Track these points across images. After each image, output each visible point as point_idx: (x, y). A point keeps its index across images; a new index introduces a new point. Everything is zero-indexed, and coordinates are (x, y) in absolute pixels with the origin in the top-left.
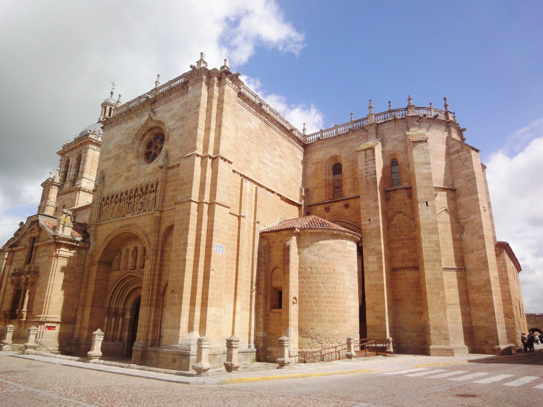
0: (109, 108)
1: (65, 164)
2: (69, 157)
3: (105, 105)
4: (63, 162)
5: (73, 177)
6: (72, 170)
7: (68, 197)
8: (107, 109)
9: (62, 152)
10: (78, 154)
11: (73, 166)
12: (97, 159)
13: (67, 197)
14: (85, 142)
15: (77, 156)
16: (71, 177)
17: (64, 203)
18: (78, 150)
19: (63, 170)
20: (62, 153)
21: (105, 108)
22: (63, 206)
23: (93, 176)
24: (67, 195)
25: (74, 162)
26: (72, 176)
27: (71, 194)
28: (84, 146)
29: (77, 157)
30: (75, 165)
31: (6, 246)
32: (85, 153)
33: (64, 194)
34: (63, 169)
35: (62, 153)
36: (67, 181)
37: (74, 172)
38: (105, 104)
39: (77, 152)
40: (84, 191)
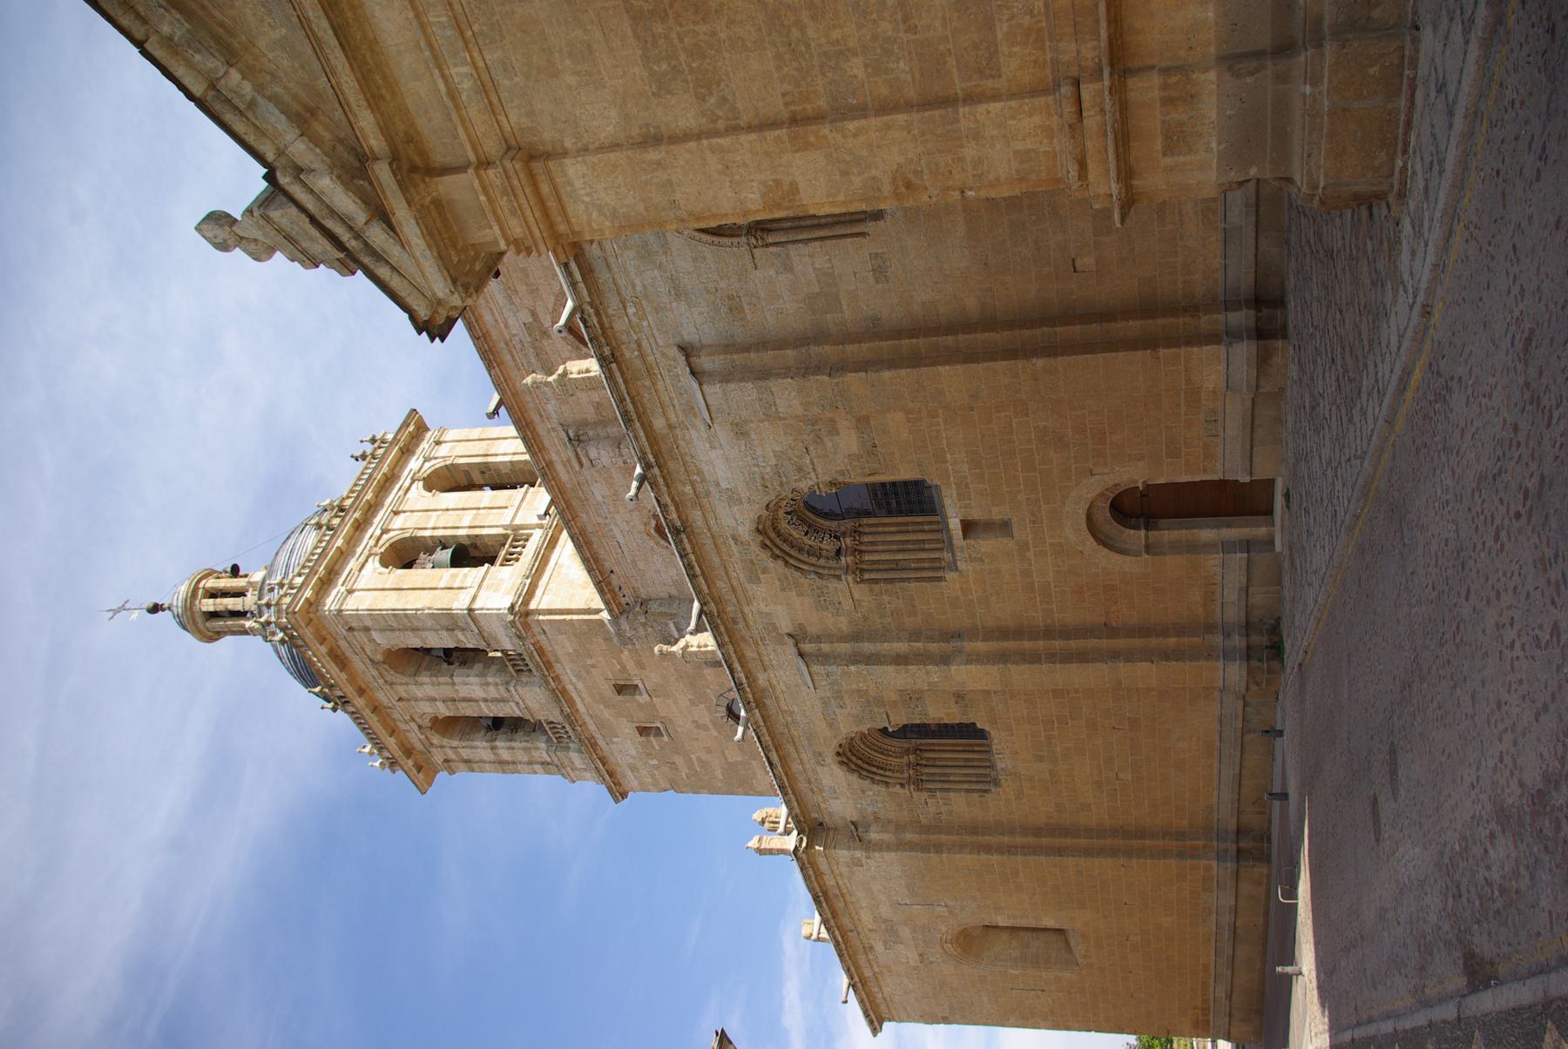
0: (205, 601)
1: (455, 743)
2: (420, 727)
3: (199, 620)
4: (451, 755)
5: (490, 679)
6: (463, 691)
7: (578, 676)
8: (211, 609)
9: (410, 763)
10: (392, 676)
11: (446, 691)
12: (392, 575)
13: (580, 685)
14: (323, 641)
15: (399, 678)
16: (493, 692)
17: (608, 691)
18: (369, 674)
19: (485, 744)
20: (423, 770)
21: (214, 615)
22: (620, 698)
23: (465, 576)
24: (569, 687)
25: (429, 690)
26: (488, 684)
27: (558, 661)
28: (343, 643)
29: (405, 680)
30: (441, 679)
31: (395, 283)
32: (367, 629)
33: (571, 703)
34: (480, 748)
35: (423, 770)
36: (518, 713)
37: (472, 679)
38: (195, 623)
39: (381, 681)
40: (530, 594)
